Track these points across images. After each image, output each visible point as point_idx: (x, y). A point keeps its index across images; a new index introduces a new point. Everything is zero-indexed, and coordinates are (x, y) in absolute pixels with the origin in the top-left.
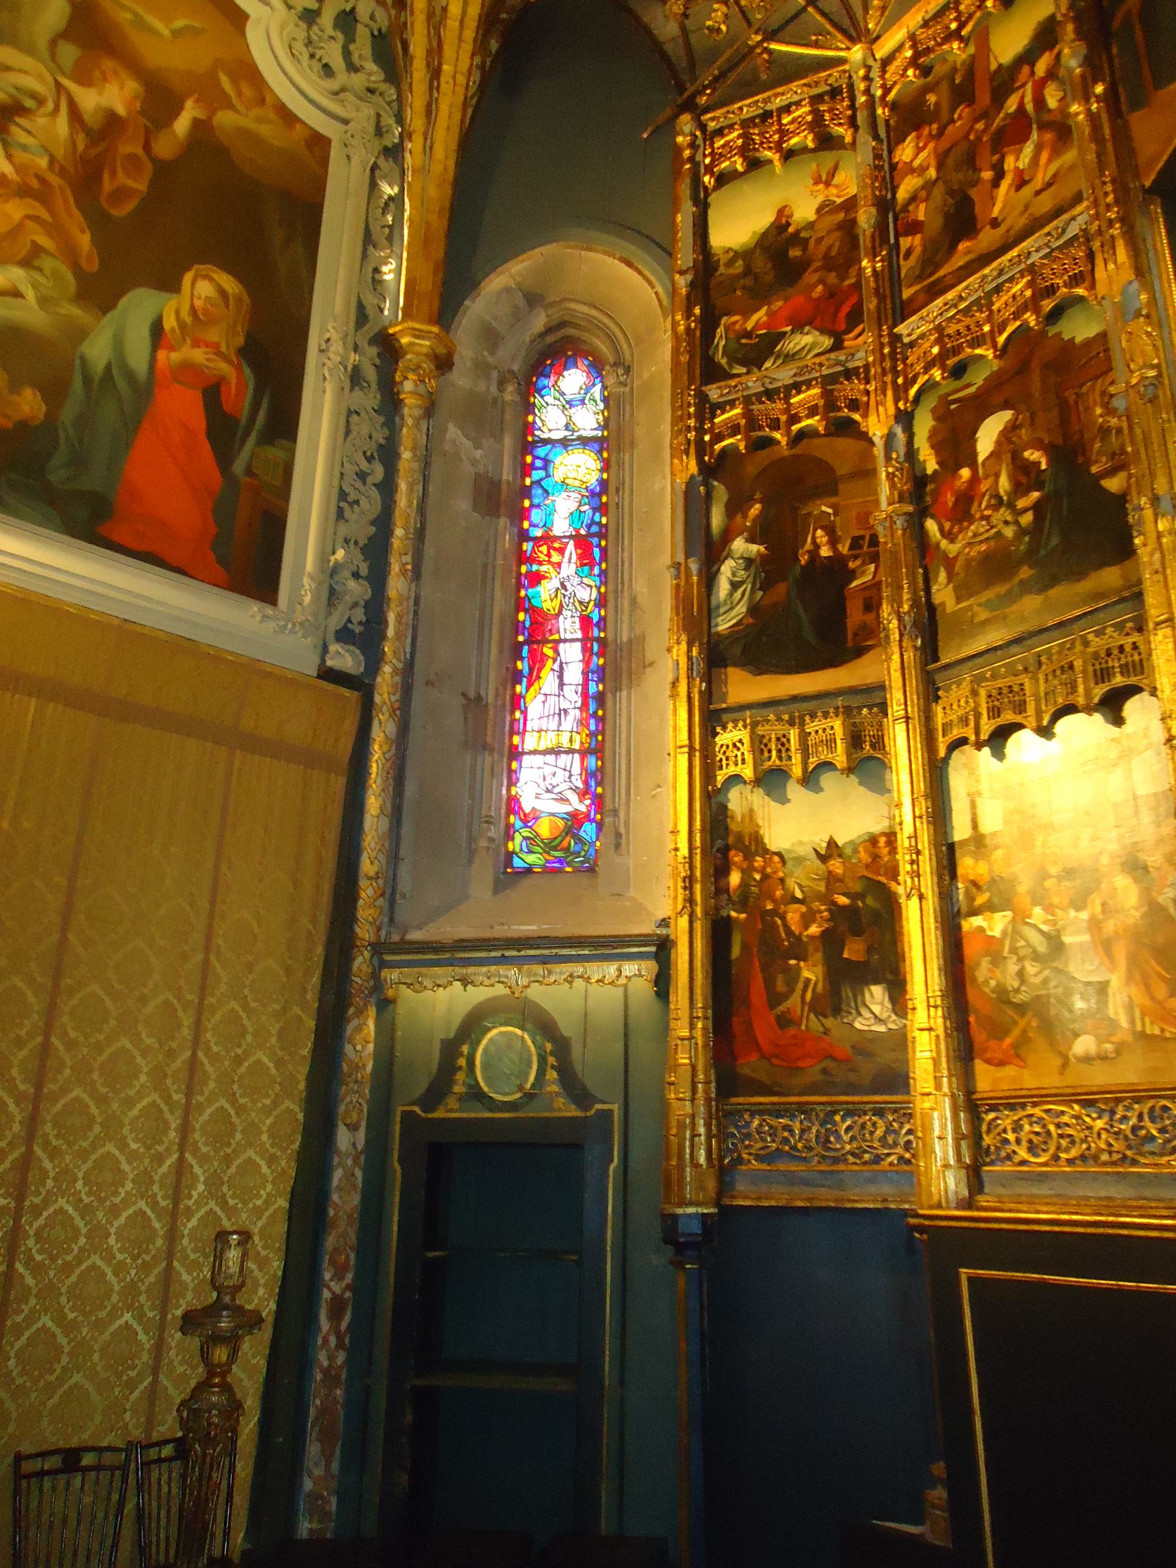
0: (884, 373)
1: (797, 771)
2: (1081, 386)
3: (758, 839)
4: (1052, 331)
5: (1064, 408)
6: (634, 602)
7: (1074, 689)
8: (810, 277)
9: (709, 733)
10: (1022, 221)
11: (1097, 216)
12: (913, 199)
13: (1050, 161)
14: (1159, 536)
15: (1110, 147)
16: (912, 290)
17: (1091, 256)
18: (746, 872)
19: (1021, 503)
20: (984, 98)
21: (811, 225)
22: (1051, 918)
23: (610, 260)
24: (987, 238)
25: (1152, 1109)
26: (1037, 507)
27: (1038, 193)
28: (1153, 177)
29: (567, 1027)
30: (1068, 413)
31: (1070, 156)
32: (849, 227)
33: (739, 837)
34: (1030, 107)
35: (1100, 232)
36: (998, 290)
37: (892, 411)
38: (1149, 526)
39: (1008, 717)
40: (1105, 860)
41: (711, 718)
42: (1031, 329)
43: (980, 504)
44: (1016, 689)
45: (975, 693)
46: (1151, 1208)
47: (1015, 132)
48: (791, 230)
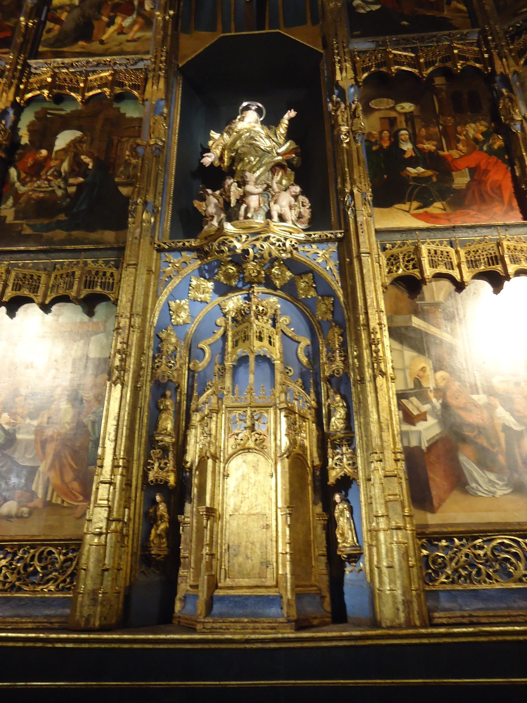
0: (14, 77)
2: (122, 137)
4: (115, 105)
7: (71, 287)
10: (116, 49)
11: (155, 63)
13: (139, 30)
14: (142, 221)
15: (169, 38)
16: (45, 49)
17: (146, 80)
19: (71, 181)
22: (12, 421)
24: (95, 46)
25: (42, 553)
27: (128, 41)
28: (184, 63)
31: (149, 34)
35: (154, 70)
36: (94, 72)
37: (11, 98)
38: (139, 214)
39: (26, 292)
40: (59, 391)
42: (106, 96)
43: (47, 172)
44: (35, 278)
45: (8, 272)
46: (22, 623)
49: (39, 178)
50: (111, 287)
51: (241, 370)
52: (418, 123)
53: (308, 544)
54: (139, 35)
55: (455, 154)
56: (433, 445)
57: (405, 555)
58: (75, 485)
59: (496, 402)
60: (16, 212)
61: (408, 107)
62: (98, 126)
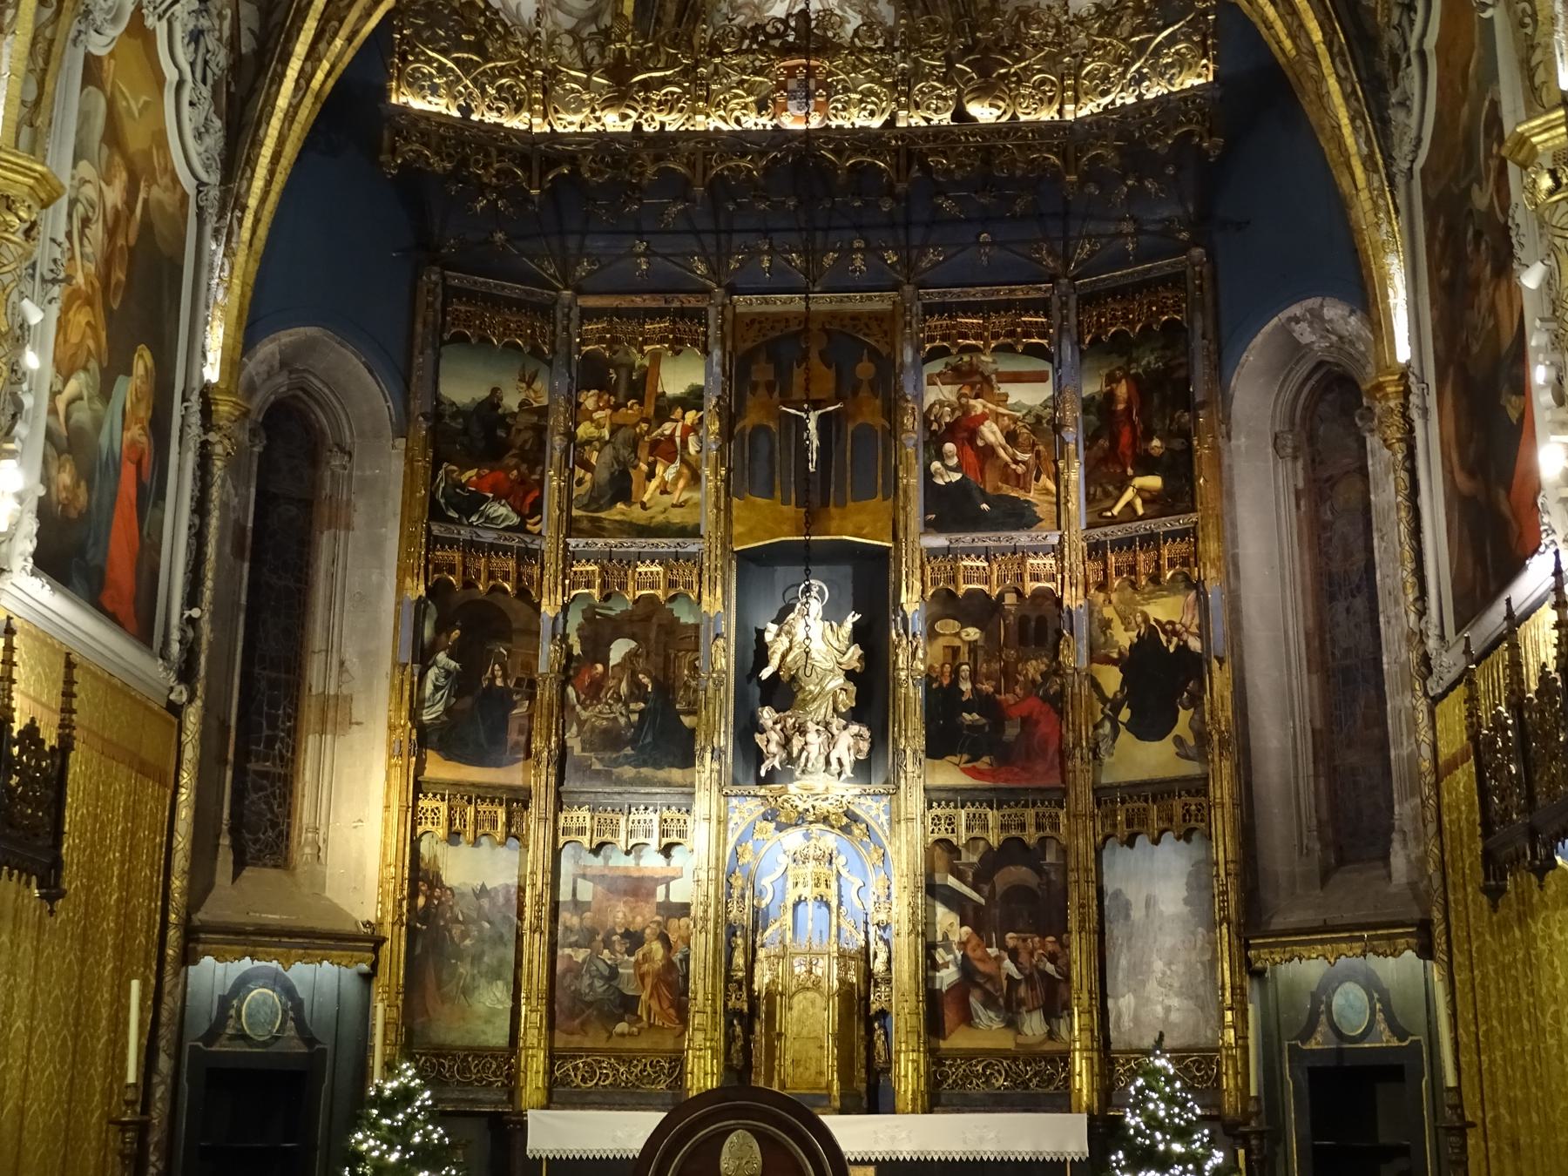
1: (470, 835)
3: (438, 876)
4: (668, 606)
5: (667, 657)
6: (342, 663)
8: (510, 460)
9: (416, 799)
10: (660, 518)
12: (589, 442)
18: (429, 899)
19: (632, 706)
20: (650, 410)
21: (514, 415)
23: (356, 361)
26: (641, 712)
27: (674, 506)
29: (302, 993)
30: (668, 663)
31: (696, 496)
32: (540, 431)
33: (427, 872)
34: (678, 440)
41: (419, 788)
47: (666, 450)
48: (500, 411)
49: (599, 702)
50: (681, 833)
51: (800, 907)
52: (981, 653)
53: (852, 1059)
54: (685, 496)
55: (1010, 698)
56: (953, 987)
57: (917, 1069)
58: (672, 1011)
59: (1005, 955)
60: (583, 742)
61: (973, 633)
62: (653, 635)
